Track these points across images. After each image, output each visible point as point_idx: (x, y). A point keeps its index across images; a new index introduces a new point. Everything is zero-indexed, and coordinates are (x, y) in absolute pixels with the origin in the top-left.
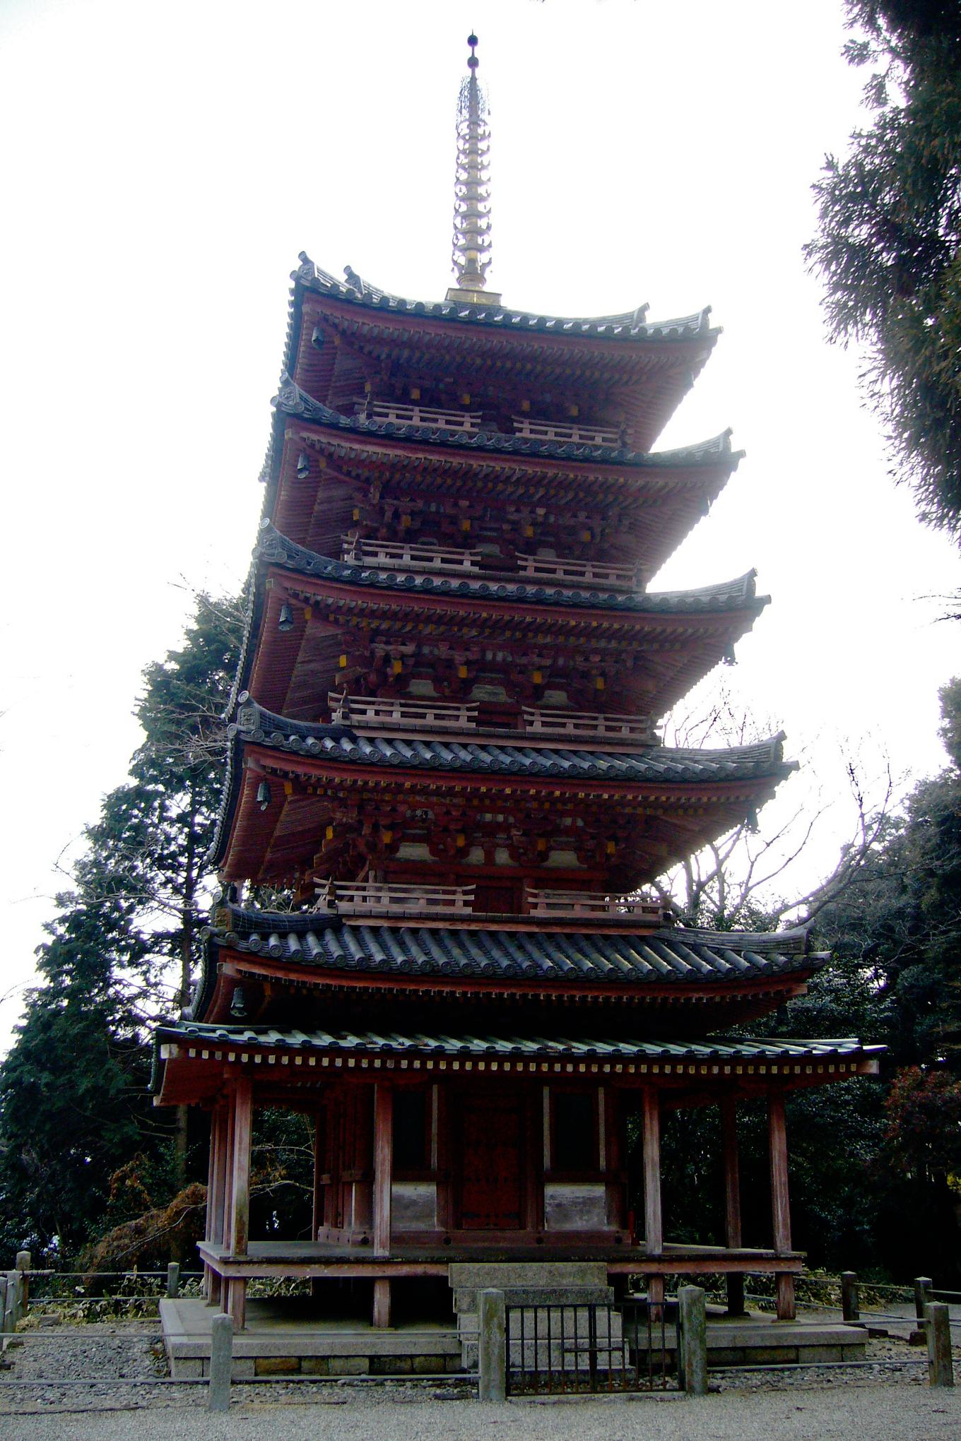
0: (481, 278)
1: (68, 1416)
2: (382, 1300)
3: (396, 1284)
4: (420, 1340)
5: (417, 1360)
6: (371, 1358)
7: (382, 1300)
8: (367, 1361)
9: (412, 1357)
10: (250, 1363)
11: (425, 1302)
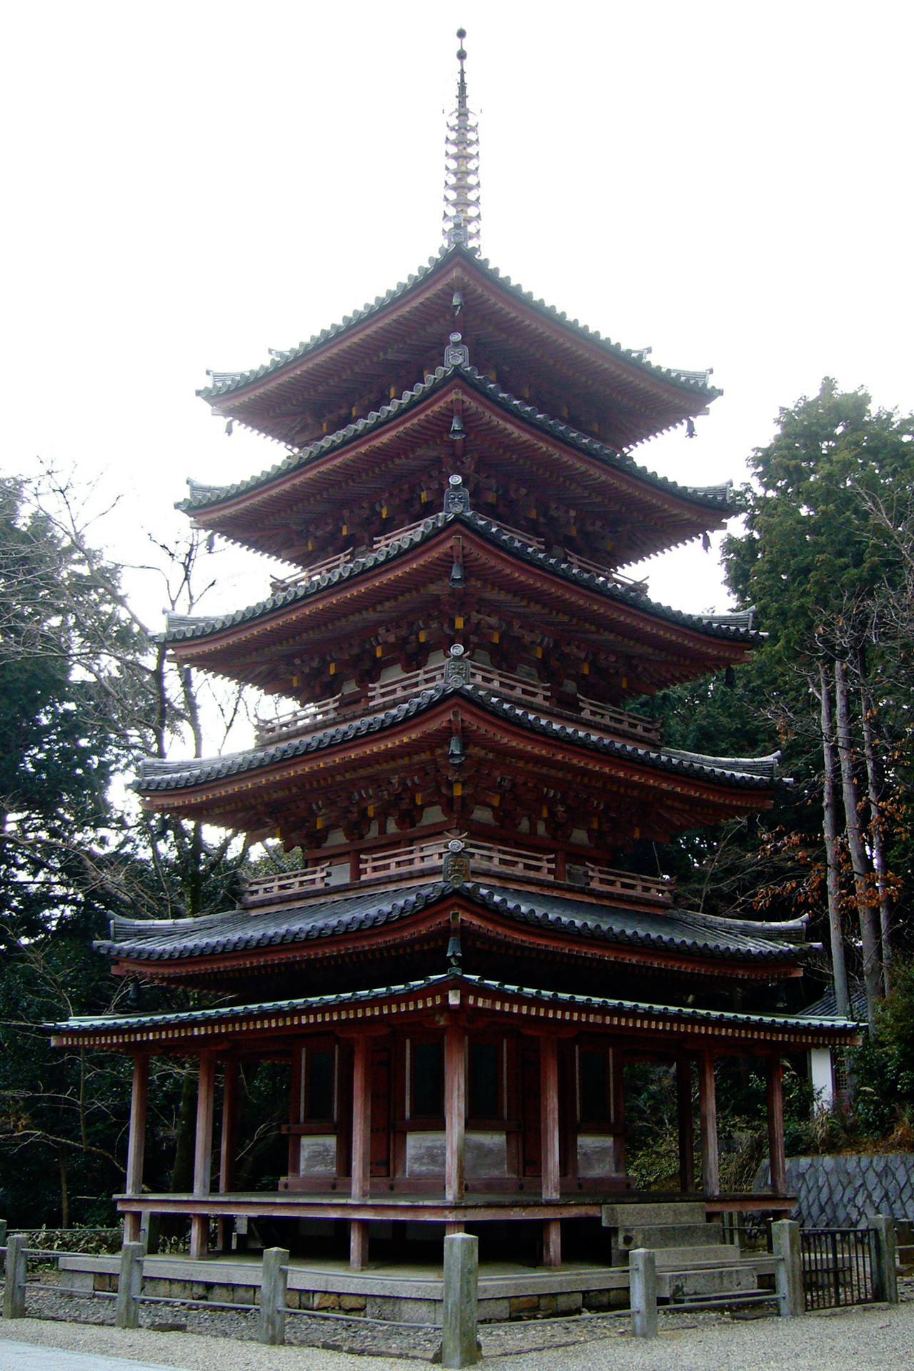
0: (833, 388)
1: (681, 1331)
2: (555, 1239)
3: (566, 1224)
4: (594, 1277)
5: (612, 1294)
6: (584, 1293)
7: (555, 1239)
8: (580, 1297)
9: (608, 1290)
10: (506, 1303)
11: (591, 1243)
